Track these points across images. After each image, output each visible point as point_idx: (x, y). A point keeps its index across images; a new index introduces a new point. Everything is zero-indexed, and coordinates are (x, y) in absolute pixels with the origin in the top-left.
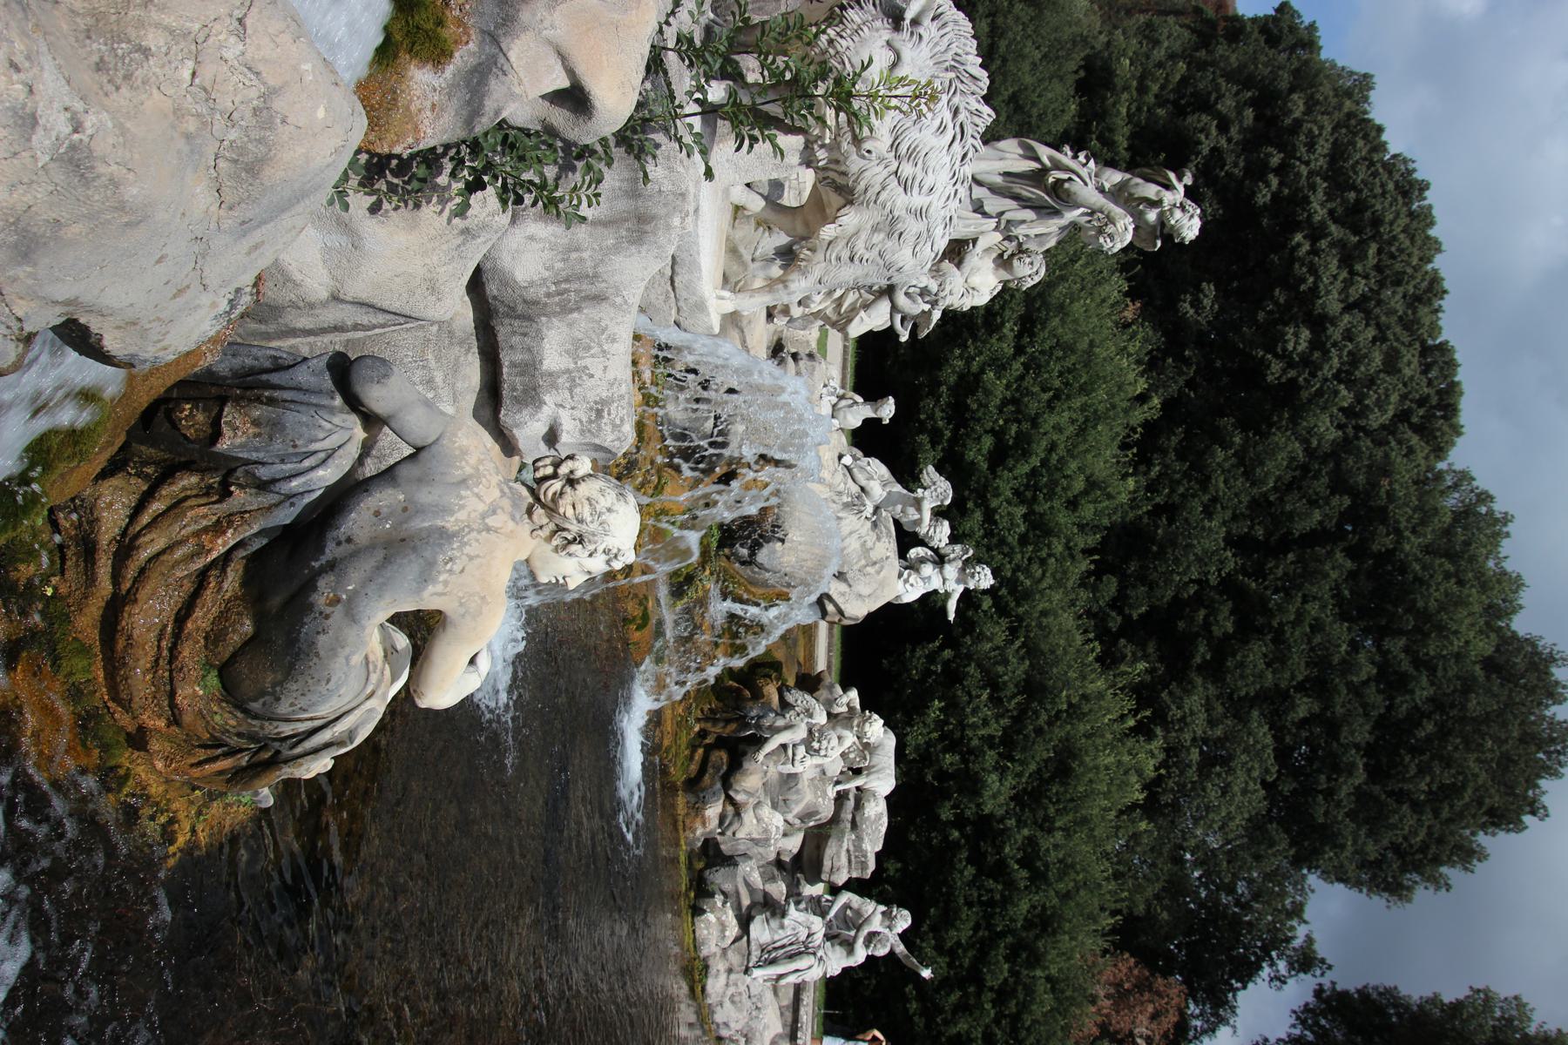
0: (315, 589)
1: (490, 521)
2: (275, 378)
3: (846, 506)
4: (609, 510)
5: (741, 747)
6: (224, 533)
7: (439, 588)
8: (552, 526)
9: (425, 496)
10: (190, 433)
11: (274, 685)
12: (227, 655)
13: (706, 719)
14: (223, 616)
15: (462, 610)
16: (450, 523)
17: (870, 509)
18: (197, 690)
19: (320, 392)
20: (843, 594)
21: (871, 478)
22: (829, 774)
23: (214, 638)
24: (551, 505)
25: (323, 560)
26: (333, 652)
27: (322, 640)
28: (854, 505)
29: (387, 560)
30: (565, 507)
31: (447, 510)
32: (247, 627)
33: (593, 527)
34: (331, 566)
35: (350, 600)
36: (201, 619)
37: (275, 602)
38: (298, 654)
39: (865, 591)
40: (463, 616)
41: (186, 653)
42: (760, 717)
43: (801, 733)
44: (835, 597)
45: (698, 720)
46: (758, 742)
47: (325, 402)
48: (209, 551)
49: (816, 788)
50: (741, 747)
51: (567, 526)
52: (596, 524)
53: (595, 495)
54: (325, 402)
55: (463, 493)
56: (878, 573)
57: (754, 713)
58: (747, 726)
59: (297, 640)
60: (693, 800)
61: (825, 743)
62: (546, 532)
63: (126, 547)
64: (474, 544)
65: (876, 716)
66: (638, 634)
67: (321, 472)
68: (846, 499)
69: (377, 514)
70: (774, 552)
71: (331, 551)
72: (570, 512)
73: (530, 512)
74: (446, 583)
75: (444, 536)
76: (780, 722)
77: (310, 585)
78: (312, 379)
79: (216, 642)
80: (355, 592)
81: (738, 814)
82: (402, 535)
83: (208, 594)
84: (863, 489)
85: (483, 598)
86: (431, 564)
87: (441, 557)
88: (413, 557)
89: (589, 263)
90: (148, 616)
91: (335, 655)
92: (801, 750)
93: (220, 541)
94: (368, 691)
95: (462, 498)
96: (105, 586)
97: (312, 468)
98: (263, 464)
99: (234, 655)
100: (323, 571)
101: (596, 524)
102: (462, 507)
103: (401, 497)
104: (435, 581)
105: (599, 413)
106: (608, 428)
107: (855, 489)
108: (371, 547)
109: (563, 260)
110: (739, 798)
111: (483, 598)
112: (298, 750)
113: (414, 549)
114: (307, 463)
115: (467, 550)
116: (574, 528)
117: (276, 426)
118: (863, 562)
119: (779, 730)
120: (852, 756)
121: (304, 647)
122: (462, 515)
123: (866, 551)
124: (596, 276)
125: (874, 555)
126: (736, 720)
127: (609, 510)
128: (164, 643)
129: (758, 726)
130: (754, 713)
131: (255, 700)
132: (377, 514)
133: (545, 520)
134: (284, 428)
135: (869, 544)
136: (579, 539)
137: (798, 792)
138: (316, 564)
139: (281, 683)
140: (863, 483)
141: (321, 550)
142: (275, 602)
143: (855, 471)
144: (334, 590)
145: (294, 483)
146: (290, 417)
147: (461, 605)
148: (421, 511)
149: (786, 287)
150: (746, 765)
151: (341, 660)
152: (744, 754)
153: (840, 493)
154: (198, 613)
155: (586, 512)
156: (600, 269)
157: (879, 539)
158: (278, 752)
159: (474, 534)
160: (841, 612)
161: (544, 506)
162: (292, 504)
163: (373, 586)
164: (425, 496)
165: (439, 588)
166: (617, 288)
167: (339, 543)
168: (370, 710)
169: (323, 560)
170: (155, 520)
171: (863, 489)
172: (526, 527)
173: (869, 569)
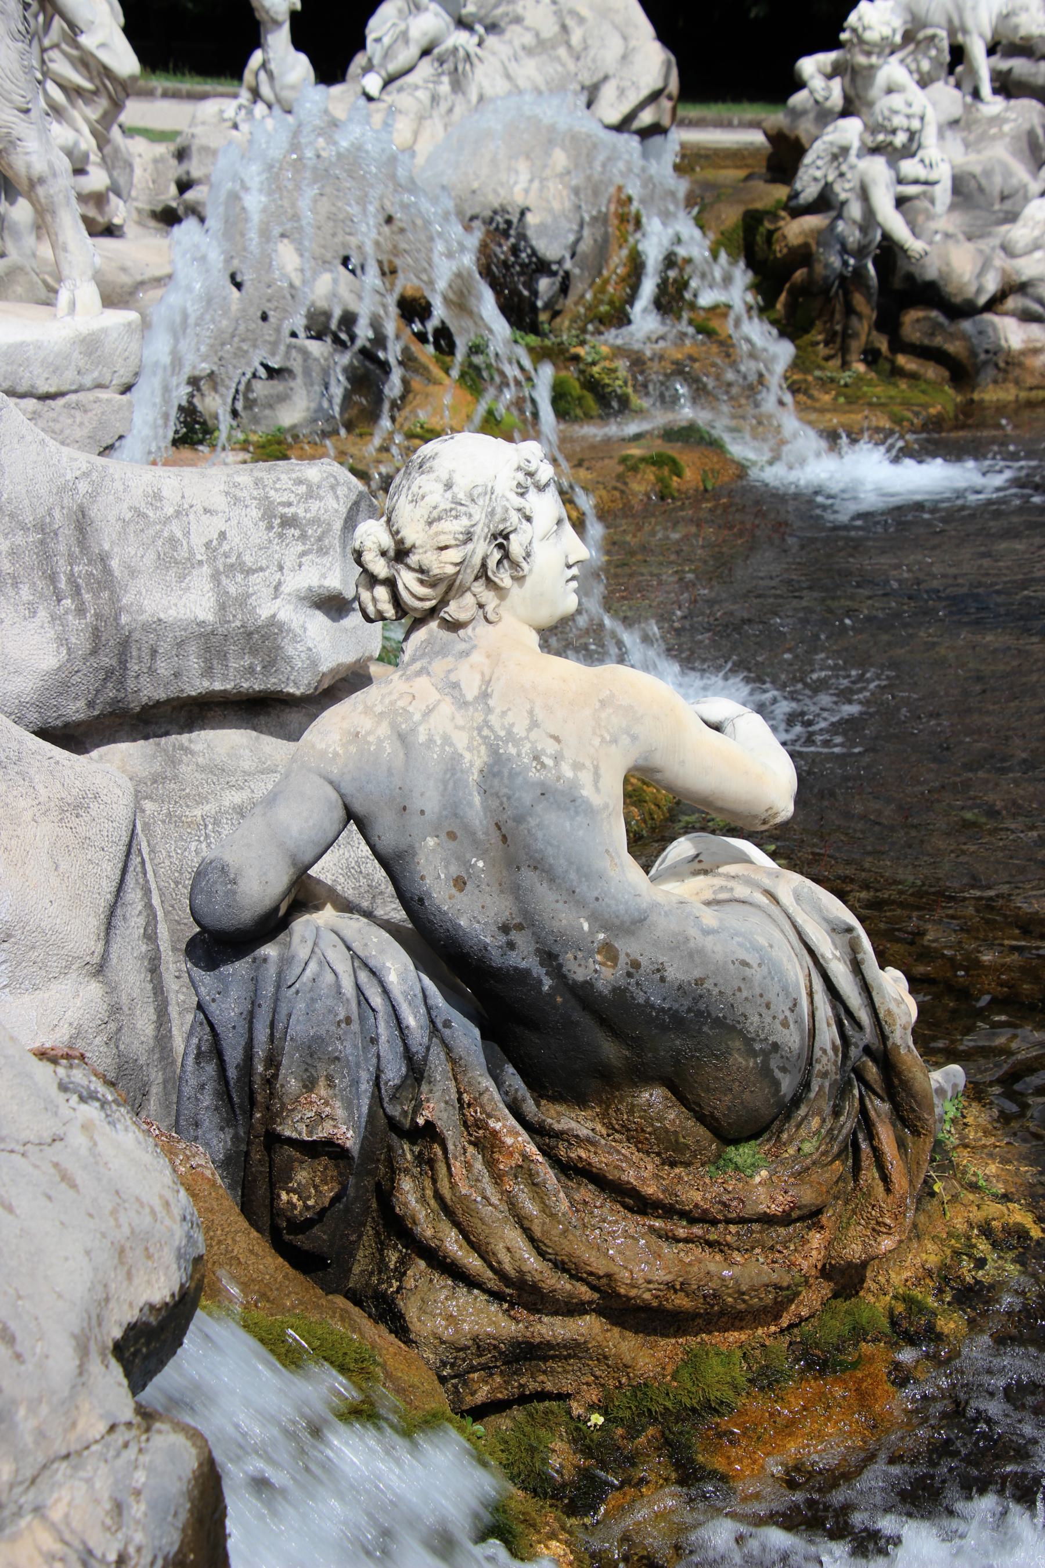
0: (588, 985)
1: (471, 692)
2: (234, 1056)
3: (458, 85)
4: (448, 486)
5: (898, 283)
6: (495, 1133)
8: (479, 587)
9: (429, 799)
10: (329, 1192)
11: (752, 1053)
12: (702, 1130)
13: (844, 350)
14: (635, 1137)
15: (625, 740)
16: (475, 760)
17: (462, 39)
18: (760, 1180)
20: (622, 92)
21: (404, 37)
22: (957, 111)
23: (672, 1153)
24: (442, 588)
25: (538, 971)
26: (694, 955)
27: (674, 973)
28: (456, 69)
29: (538, 865)
30: (443, 564)
31: (453, 766)
33: (479, 514)
34: (549, 958)
35: (606, 927)
36: (642, 1173)
37: (611, 1051)
38: (699, 1013)
39: (615, 47)
40: (634, 738)
41: (697, 1197)
42: (844, 250)
43: (877, 168)
44: (626, 108)
45: (845, 365)
46: (889, 252)
47: (272, 970)
48: (525, 1157)
49: (983, 137)
50: (898, 283)
51: (477, 561)
52: (474, 509)
53: (422, 511)
54: (272, 970)
55: (422, 738)
56: (581, 20)
57: (835, 261)
58: (859, 273)
59: (675, 1015)
60: (991, 372)
61: (898, 121)
62: (489, 597)
63: (520, 1294)
64: (510, 718)
65: (852, 19)
66: (688, 474)
67: (392, 978)
68: (445, 87)
69: (460, 883)
70: (542, 228)
71: (524, 957)
72: (454, 555)
73: (454, 626)
74: (577, 766)
75: (497, 771)
76: (855, 210)
77: (583, 994)
78: (234, 994)
79: (679, 1148)
81: (1022, 288)
82: (495, 837)
83: (599, 1160)
84: (426, 52)
85: (603, 703)
87: (533, 775)
88: (533, 822)
89: (19, 539)
90: (634, 1256)
91: (701, 951)
92: (909, 167)
93: (509, 1141)
94: (764, 900)
95: (431, 740)
96: (587, 1327)
97: (386, 992)
98: (379, 1071)
99: (701, 1119)
100: (557, 972)
101: (474, 509)
102: (447, 740)
103: (431, 842)
104: (574, 785)
105: (288, 522)
106: (315, 506)
107: (426, 68)
108: (516, 891)
109: (15, 585)
110: (991, 285)
111: (603, 703)
112: (864, 1016)
113: (519, 819)
114: (377, 1000)
115: (520, 730)
116: (481, 548)
117: (314, 1050)
118: (562, 52)
119: (869, 212)
120: (926, 65)
121: (687, 1003)
122: (461, 740)
123: (541, 46)
124: (41, 527)
125: (549, 29)
126: (847, 294)
127: (448, 486)
128: (681, 1232)
129: (861, 252)
130: (835, 261)
131: (776, 1084)
132: (460, 883)
133: (469, 599)
134: (318, 1039)
135: (529, 39)
136: (501, 538)
137: (988, 173)
138: (547, 984)
139: (748, 1041)
140: (414, 51)
141: (522, 976)
142: (611, 1051)
143: (392, 67)
144: (591, 954)
146: (299, 1028)
147: (615, 741)
148: (454, 810)
149: (41, 180)
150: (931, 272)
151: (709, 942)
152: (910, 277)
153: (435, 99)
154: (630, 1176)
155: (451, 528)
157: (518, 20)
158: (867, 1050)
159: (493, 719)
160: (655, 96)
161: (444, 602)
162: (447, 1024)
163: (583, 889)
165: (585, 777)
166: (62, 490)
167: (511, 945)
168: (798, 897)
169: (538, 971)
170: (475, 1246)
171: (426, 52)
172: (479, 631)
173: (576, 38)
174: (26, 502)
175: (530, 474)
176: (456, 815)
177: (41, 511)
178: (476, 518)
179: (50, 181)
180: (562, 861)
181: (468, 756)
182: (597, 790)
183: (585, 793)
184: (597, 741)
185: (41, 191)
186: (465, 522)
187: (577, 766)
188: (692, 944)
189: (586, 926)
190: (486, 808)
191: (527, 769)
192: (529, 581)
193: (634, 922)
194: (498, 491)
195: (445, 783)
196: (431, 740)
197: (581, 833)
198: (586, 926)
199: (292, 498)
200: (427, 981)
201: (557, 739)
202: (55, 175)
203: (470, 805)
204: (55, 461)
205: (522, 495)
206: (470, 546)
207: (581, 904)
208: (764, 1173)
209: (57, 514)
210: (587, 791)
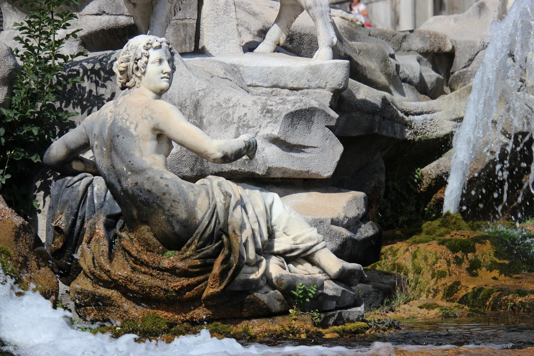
7: (133, 126)
10: (61, 244)
15: (149, 118)
16: (109, 121)
18: (170, 259)
19: (61, 186)
23: (148, 247)
24: (125, 75)
31: (104, 122)
32: (144, 228)
33: (132, 54)
36: (135, 248)
40: (152, 118)
47: (66, 182)
51: (131, 67)
63: (97, 280)
67: (95, 189)
72: (124, 65)
75: (114, 123)
79: (149, 245)
80: (127, 167)
86: (121, 129)
87: (119, 124)
90: (120, 269)
91: (158, 182)
93: (97, 231)
95: (103, 115)
97: (92, 193)
102: (106, 115)
104: (129, 128)
111: (146, 107)
115: (121, 113)
116: (131, 63)
128: (143, 270)
145: (96, 201)
147: (146, 118)
151: (161, 181)
156: (176, 101)
164: (96, 131)
166: (192, 94)
172: (134, 90)
174: (177, 96)
175: (151, 44)
176: (101, 135)
177: (182, 99)
178: (131, 55)
179: (314, 8)
180: (121, 149)
181: (109, 119)
182: (135, 130)
183: (131, 130)
184: (140, 117)
185: (310, 11)
186: (127, 55)
187: (131, 123)
188: (155, 180)
189: (125, 169)
190: (109, 133)
191: (118, 122)
192: (146, 74)
193: (140, 171)
194: (139, 48)
195: (101, 126)
196: (103, 115)
197: (128, 142)
198: (125, 169)
199: (274, 103)
200: (109, 192)
201: (129, 115)
202: (316, 6)
203: (105, 132)
204: (193, 84)
205: (147, 50)
206: (129, 63)
207: (123, 161)
208: (172, 258)
209: (188, 101)
210: (132, 130)
